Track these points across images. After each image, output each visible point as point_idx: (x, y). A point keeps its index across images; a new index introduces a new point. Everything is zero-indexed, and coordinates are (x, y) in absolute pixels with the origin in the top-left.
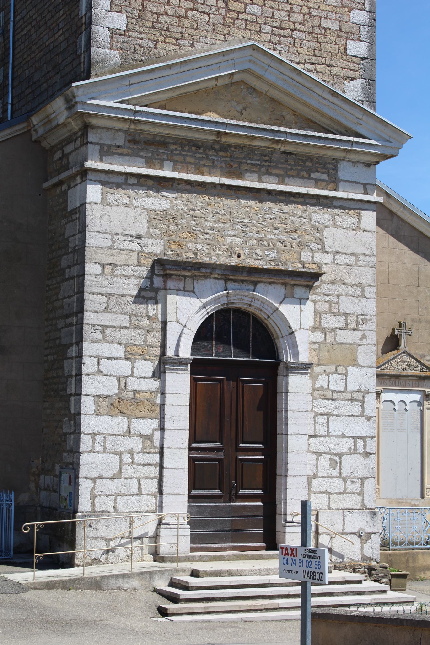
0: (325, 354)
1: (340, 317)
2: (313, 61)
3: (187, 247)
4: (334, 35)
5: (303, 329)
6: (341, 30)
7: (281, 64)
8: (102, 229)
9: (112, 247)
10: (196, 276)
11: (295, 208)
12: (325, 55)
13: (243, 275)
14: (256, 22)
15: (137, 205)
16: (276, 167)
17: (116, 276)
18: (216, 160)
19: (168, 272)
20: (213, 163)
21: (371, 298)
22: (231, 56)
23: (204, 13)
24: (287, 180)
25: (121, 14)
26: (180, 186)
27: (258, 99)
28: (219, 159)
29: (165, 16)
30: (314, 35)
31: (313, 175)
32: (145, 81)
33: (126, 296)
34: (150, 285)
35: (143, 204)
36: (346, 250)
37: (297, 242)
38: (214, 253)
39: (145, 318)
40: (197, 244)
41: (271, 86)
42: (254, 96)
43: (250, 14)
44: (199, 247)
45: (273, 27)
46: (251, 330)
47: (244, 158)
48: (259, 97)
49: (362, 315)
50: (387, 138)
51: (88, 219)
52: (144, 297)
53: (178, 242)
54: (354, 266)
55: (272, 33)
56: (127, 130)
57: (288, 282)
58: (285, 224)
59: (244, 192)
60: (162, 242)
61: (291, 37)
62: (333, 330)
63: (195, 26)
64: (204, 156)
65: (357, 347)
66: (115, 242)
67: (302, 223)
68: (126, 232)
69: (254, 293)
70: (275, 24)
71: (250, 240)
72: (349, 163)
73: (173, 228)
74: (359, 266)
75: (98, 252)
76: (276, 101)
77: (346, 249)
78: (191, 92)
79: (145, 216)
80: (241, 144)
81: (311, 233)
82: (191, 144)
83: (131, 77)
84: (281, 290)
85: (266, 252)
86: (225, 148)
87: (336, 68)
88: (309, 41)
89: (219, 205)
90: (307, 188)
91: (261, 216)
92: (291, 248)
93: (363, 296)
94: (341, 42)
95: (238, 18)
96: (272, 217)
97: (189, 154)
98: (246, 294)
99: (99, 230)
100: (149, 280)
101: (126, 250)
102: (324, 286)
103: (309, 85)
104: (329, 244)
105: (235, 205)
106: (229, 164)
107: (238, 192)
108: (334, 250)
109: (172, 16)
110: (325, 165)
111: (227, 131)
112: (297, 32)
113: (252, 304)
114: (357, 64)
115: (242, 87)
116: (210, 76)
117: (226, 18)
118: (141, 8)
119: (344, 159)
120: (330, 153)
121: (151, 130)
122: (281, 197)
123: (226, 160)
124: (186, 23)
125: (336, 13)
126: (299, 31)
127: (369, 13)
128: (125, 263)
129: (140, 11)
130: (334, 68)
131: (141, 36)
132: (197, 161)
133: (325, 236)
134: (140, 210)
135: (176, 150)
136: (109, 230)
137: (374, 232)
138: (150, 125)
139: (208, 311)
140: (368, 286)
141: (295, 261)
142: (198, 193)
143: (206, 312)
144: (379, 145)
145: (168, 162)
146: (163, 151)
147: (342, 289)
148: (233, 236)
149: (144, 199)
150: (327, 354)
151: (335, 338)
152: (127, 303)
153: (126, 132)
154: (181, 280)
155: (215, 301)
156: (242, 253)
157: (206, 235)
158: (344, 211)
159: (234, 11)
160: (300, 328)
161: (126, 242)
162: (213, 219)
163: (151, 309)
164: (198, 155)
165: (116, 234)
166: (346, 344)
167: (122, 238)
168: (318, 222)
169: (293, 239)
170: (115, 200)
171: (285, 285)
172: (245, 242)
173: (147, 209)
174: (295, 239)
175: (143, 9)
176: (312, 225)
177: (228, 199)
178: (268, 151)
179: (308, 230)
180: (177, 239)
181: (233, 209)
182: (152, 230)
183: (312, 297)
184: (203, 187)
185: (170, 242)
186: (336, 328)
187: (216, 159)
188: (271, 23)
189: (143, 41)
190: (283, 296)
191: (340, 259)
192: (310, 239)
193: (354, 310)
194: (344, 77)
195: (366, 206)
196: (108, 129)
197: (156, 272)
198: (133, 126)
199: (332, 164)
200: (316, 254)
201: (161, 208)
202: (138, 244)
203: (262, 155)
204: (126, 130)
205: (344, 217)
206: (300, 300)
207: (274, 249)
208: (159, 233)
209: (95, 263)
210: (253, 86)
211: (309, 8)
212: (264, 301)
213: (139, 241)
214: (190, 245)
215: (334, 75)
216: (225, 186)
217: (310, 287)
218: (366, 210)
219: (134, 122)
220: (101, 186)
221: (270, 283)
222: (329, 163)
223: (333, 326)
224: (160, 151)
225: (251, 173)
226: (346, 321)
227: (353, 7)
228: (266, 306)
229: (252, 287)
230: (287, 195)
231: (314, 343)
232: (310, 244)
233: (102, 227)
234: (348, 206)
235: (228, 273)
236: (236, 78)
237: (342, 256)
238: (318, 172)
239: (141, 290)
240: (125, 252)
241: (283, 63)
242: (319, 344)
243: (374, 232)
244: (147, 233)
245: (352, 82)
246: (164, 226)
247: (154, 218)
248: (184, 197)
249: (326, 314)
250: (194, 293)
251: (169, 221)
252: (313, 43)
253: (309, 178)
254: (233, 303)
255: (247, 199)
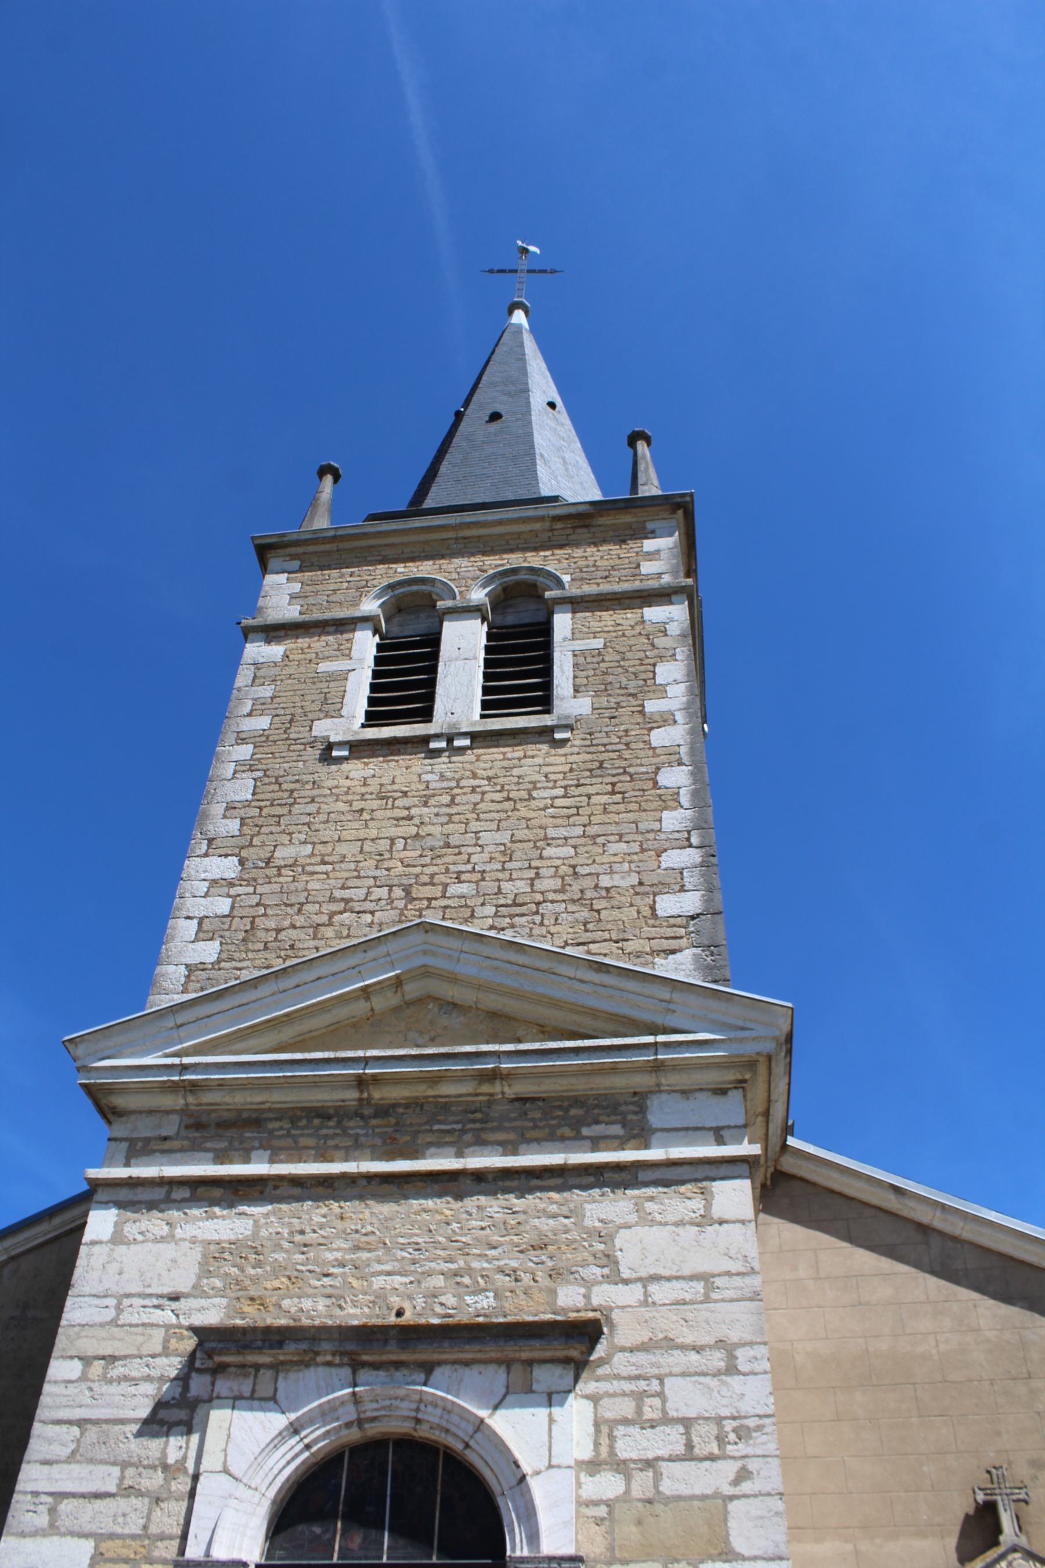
0: (628, 1532)
1: (667, 1429)
2: (581, 940)
3: (280, 1306)
4: (627, 893)
5: (559, 1467)
6: (641, 883)
7: (482, 942)
8: (101, 1289)
9: (114, 1323)
10: (283, 1363)
11: (541, 1199)
12: (609, 927)
13: (389, 1348)
14: (466, 906)
15: (184, 1236)
16: (499, 1129)
17: (110, 1381)
18: (363, 1135)
19: (218, 1359)
20: (356, 1140)
21: (756, 1374)
22: (382, 949)
23: (364, 912)
24: (523, 1147)
25: (211, 942)
26: (278, 1192)
27: (462, 1019)
28: (370, 1131)
29: (291, 931)
30: (584, 902)
31: (585, 1131)
32: (208, 1017)
33: (122, 1422)
34: (181, 1394)
35: (195, 1233)
36: (678, 1271)
37: (548, 1269)
38: (342, 1313)
39: (155, 1471)
40: (302, 1299)
41: (479, 989)
42: (454, 1015)
43: (454, 897)
44: (307, 1304)
45: (497, 906)
46: (439, 1488)
47: (425, 1123)
48: (465, 1015)
49: (734, 1418)
50: (740, 1023)
51: (78, 1272)
52: (162, 1423)
53: (260, 1298)
54: (702, 1302)
55: (496, 915)
56: (184, 1108)
57: (512, 1355)
58: (517, 1235)
59: (420, 1184)
60: (224, 1301)
61: (537, 913)
62: (649, 1464)
63: (345, 933)
64: (338, 1131)
65: (725, 1506)
66: (123, 1311)
67: (560, 1228)
68: (149, 1291)
69: (424, 1388)
70: (502, 901)
71: (429, 1278)
72: (674, 1094)
73: (252, 1272)
74: (716, 1301)
75: (83, 1334)
76: (501, 1016)
77: (675, 1268)
78: (322, 1028)
79: (197, 1254)
80: (417, 1098)
81: (584, 1246)
82: (313, 1114)
83: (177, 1011)
84: (498, 1377)
85: (466, 1298)
86: (384, 1111)
87: (635, 942)
88: (573, 913)
89: (361, 1216)
90: (563, 1155)
91: (459, 1225)
92: (532, 1283)
93: (731, 1369)
94: (643, 903)
95: (428, 907)
96: (483, 1224)
97: (306, 1131)
98: (401, 1392)
99: (94, 1292)
100: (181, 1383)
101: (144, 1325)
102: (619, 1358)
103: (545, 965)
104: (628, 1263)
105: (398, 1212)
106: (391, 1138)
107: (405, 1186)
108: (643, 1274)
109: (304, 927)
110: (616, 1108)
111: (367, 1071)
112: (549, 904)
113: (420, 1416)
114: (680, 927)
115: (431, 1006)
116: (342, 989)
117: (406, 912)
118: (248, 927)
119: (658, 1090)
120: (619, 1083)
121: (228, 1099)
122: (508, 1183)
123: (386, 1132)
124: (329, 932)
125: (630, 862)
126: (552, 902)
127: (699, 850)
128: (135, 1352)
129: (246, 931)
130: (630, 943)
131: (239, 965)
132: (322, 1141)
133: (618, 1247)
134: (187, 1244)
135: (281, 1128)
136: (115, 1289)
137: (750, 1221)
138: (222, 1089)
139: (306, 1441)
140: (744, 1344)
141: (542, 1309)
142: (316, 1199)
143: (301, 1446)
144: (722, 1040)
145: (261, 1152)
146: (255, 1135)
147: (671, 1360)
148: (389, 1274)
149: (201, 1224)
150: (634, 1529)
151: (656, 1486)
152: (121, 1438)
153: (184, 1112)
154: (246, 1376)
155: (325, 1413)
156: (407, 1306)
157: (325, 1279)
158: (666, 1190)
159: (421, 899)
160: (550, 1466)
161: (147, 1310)
162: (345, 1246)
163: (175, 1447)
164: (324, 1131)
165: (128, 1296)
166: (692, 1498)
167: (137, 1302)
168: (601, 1221)
169: (538, 1264)
170: (139, 1233)
171: (508, 1364)
172: (416, 1283)
173: (202, 1241)
174: (543, 1263)
175: (252, 928)
176: (584, 1227)
177: (382, 1202)
178: (481, 1102)
179: (574, 1241)
180: (259, 1293)
181: (391, 1219)
182: (205, 1281)
183: (587, 1386)
184: (327, 1187)
185: (242, 1300)
186: (658, 1459)
187: (361, 1132)
188: (495, 901)
189: (243, 971)
190: (503, 1390)
191: (660, 1292)
192: (580, 1259)
193: (710, 1408)
194: (654, 951)
195: (724, 1170)
196: (151, 1112)
197: (198, 1364)
198: (191, 1099)
199: (633, 1103)
200: (596, 1289)
201: (233, 1238)
202: (172, 1311)
203: (466, 1112)
204: (182, 1109)
205: (666, 1201)
206: (550, 1395)
207: (486, 1290)
208: (218, 1283)
209: (72, 1358)
210: (450, 1000)
211: (574, 867)
212: (449, 1407)
213: (175, 1305)
214: (286, 1303)
215: (629, 954)
216: (378, 1180)
217: (579, 1367)
218: (722, 1179)
219: (191, 1091)
220: (117, 1211)
221: (467, 1364)
222: (626, 1103)
223: (650, 1455)
224: (247, 1135)
225: (438, 1147)
226: (687, 1439)
227: (665, 847)
228: (455, 1419)
229: (422, 1377)
230: (523, 1177)
231: (596, 1503)
232: (580, 1269)
233: (102, 1285)
234: (675, 1178)
235: (350, 1347)
236: (412, 990)
237: (667, 1284)
238: (597, 1122)
239: (160, 1405)
240: (140, 1329)
241: (485, 940)
242: (608, 1503)
243: (750, 1221)
244: (194, 1287)
245: (671, 957)
246: (235, 1270)
247: (215, 1257)
248: (286, 1210)
249: (629, 1425)
250: (276, 1402)
251: (246, 1258)
252: (582, 914)
253: (578, 1137)
254: (374, 1419)
255: (426, 1197)
